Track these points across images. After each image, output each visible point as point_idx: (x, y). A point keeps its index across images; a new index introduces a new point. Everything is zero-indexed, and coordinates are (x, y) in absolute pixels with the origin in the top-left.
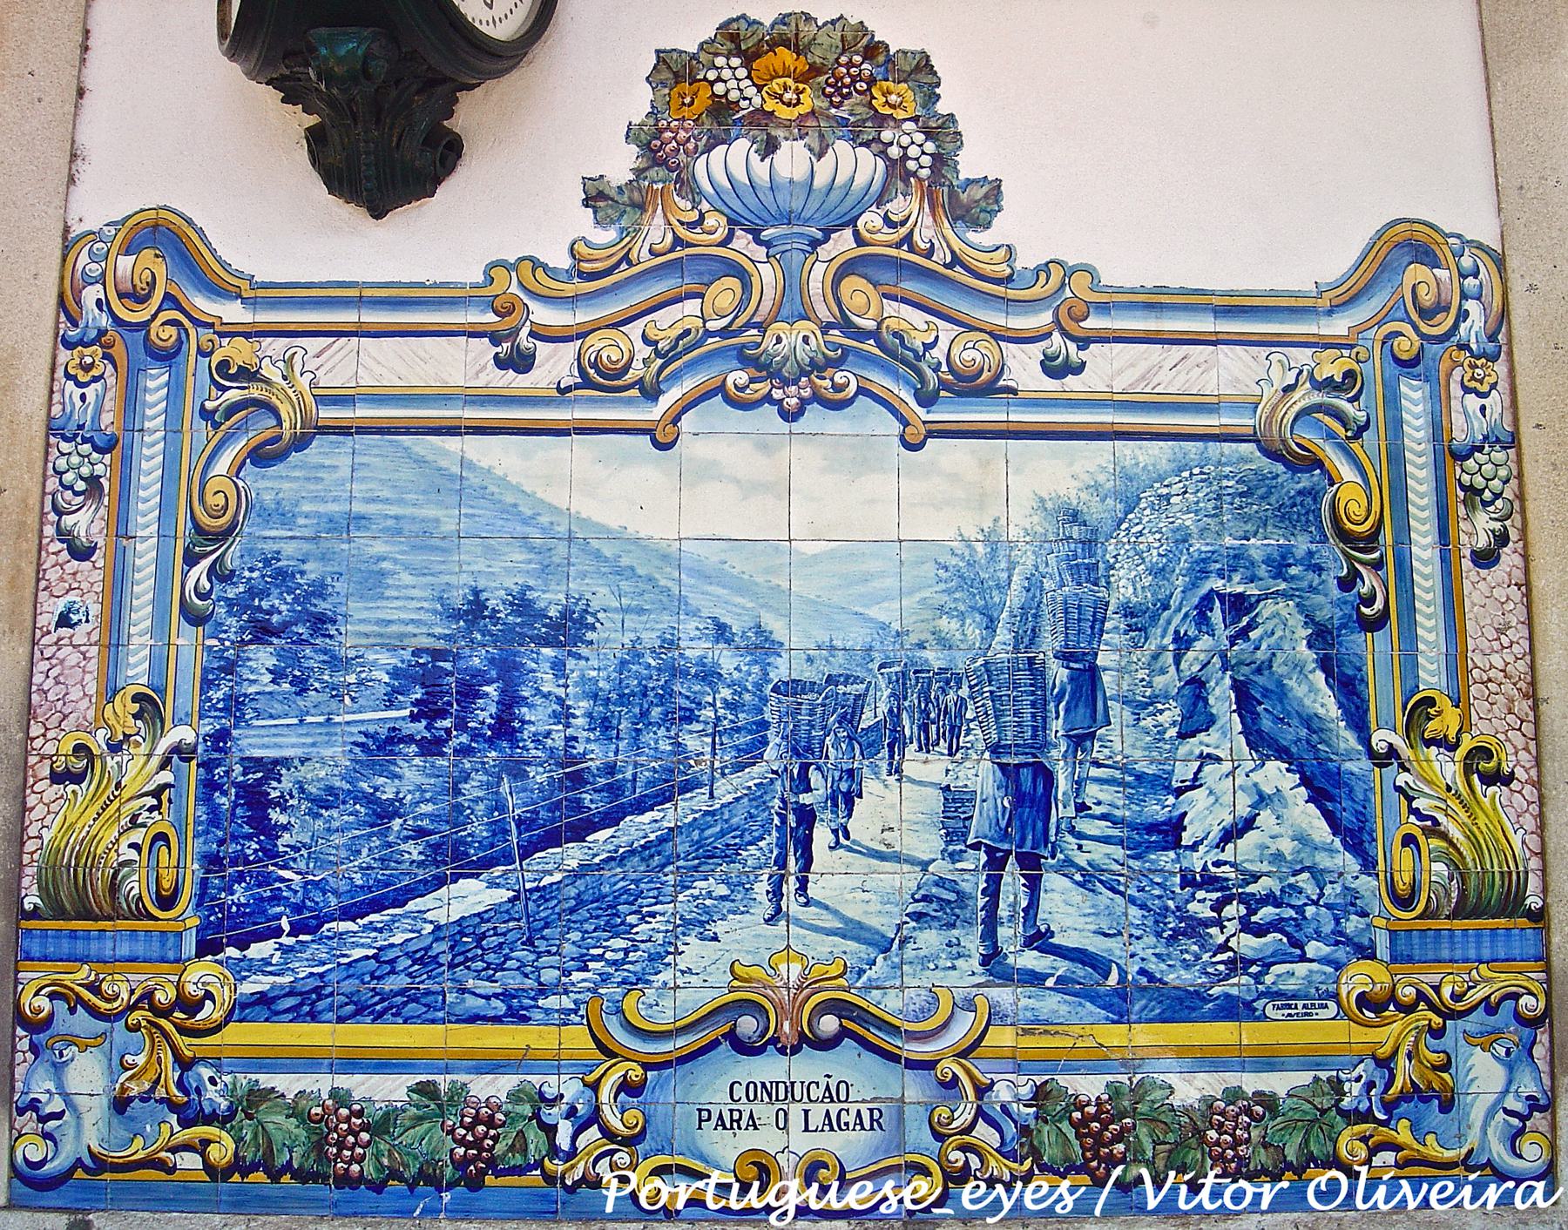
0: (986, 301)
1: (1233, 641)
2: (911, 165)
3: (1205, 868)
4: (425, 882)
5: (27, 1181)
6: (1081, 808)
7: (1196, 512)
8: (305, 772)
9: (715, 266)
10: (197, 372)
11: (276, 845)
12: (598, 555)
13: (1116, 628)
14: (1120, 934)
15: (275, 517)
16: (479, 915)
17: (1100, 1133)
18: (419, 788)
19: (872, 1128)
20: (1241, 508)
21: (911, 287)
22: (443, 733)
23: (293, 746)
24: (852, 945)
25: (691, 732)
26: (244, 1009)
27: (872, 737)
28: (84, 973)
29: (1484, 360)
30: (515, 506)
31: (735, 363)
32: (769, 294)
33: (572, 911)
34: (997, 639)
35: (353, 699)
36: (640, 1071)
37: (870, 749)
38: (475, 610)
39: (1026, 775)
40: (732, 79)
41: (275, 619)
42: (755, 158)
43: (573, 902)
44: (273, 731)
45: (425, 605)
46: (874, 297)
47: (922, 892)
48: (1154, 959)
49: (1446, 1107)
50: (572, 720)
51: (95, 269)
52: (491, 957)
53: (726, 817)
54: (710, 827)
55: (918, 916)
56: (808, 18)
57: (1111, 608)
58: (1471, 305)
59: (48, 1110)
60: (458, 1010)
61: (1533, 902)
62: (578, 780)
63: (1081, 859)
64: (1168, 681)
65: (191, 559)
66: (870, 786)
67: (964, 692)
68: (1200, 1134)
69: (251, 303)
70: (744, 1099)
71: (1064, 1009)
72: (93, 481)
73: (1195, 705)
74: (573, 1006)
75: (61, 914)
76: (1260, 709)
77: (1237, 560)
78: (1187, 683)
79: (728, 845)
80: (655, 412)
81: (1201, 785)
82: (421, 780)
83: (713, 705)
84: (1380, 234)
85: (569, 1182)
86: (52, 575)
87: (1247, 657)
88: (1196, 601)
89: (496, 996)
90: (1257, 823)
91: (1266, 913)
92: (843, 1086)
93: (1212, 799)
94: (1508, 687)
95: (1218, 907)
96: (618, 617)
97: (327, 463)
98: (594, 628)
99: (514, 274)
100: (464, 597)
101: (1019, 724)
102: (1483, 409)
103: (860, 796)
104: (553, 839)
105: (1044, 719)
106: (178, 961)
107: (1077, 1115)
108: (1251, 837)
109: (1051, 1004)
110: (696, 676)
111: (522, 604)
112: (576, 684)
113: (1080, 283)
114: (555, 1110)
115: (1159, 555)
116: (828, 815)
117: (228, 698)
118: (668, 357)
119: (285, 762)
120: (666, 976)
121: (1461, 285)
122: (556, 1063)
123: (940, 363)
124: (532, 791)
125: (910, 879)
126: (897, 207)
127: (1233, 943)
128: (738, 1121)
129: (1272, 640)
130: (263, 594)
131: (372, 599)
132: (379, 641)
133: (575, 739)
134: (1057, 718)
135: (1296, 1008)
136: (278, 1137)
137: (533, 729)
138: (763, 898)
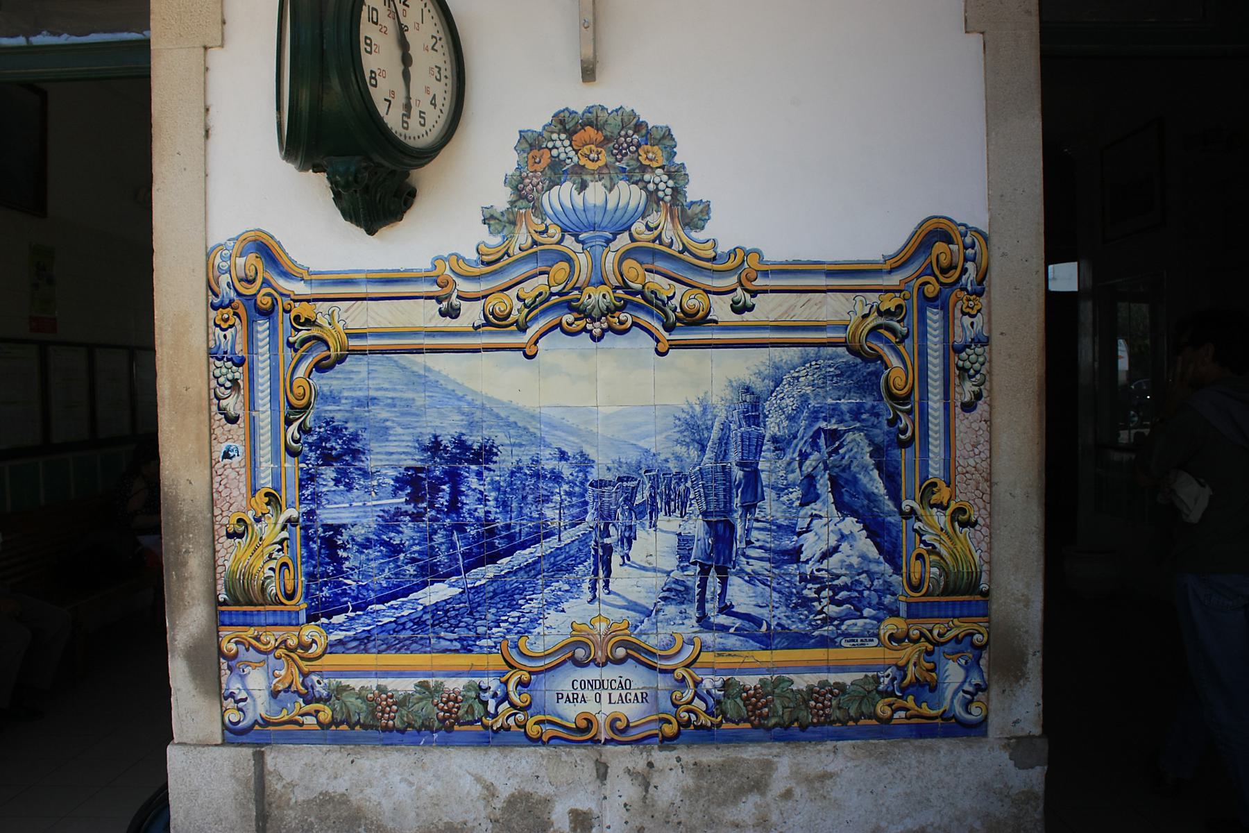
0: (701, 272)
1: (830, 455)
2: (661, 194)
3: (812, 572)
4: (417, 584)
5: (231, 731)
6: (749, 543)
7: (813, 386)
8: (354, 531)
9: (554, 256)
10: (283, 321)
12: (498, 416)
13: (769, 449)
14: (767, 606)
15: (330, 399)
16: (445, 601)
18: (412, 538)
19: (642, 702)
20: (837, 383)
21: (660, 265)
22: (422, 510)
23: (347, 518)
24: (632, 614)
25: (548, 508)
26: (331, 648)
27: (641, 508)
28: (252, 631)
29: (974, 296)
30: (454, 391)
31: (567, 310)
32: (584, 270)
33: (491, 598)
34: (706, 456)
35: (376, 493)
36: (528, 675)
37: (640, 515)
38: (435, 447)
39: (720, 526)
40: (562, 147)
41: (334, 453)
42: (575, 193)
43: (491, 594)
44: (337, 510)
45: (410, 444)
46: (641, 271)
47: (667, 587)
48: (785, 618)
49: (933, 689)
50: (487, 503)
51: (225, 265)
52: (452, 621)
53: (567, 550)
54: (559, 555)
55: (665, 599)
56: (603, 108)
57: (766, 439)
58: (970, 265)
59: (239, 697)
60: (437, 647)
61: (984, 587)
62: (492, 533)
63: (748, 569)
64: (796, 476)
65: (289, 423)
66: (640, 533)
67: (689, 484)
68: (806, 702)
69: (309, 282)
70: (579, 688)
71: (738, 643)
72: (234, 381)
73: (809, 489)
74: (493, 644)
75: (237, 603)
76: (843, 490)
77: (835, 411)
78: (805, 477)
79: (568, 565)
80: (524, 339)
81: (811, 531)
82: (413, 534)
83: (559, 493)
84: (921, 225)
85: (495, 728)
86: (218, 432)
87: (837, 463)
88: (811, 433)
89: (456, 640)
90: (840, 549)
91: (843, 594)
92: (628, 682)
93: (817, 537)
94: (977, 476)
95: (818, 592)
96: (509, 448)
97: (355, 370)
98: (497, 455)
99: (447, 263)
100: (430, 439)
101: (717, 501)
102: (972, 324)
103: (635, 539)
105: (731, 497)
106: (298, 625)
107: (745, 695)
108: (837, 557)
109: (732, 641)
110: (550, 478)
111: (460, 443)
112: (489, 484)
113: (752, 261)
114: (487, 694)
115: (793, 409)
116: (619, 549)
117: (313, 494)
118: (531, 307)
119: (344, 526)
120: (539, 629)
121: (965, 254)
123: (676, 308)
124: (469, 539)
125: (659, 581)
126: (653, 219)
127: (825, 610)
128: (576, 699)
129: (851, 454)
130: (327, 440)
131: (383, 441)
132: (387, 463)
133: (490, 512)
134: (737, 496)
136: (352, 708)
137: (468, 507)
138: (587, 591)
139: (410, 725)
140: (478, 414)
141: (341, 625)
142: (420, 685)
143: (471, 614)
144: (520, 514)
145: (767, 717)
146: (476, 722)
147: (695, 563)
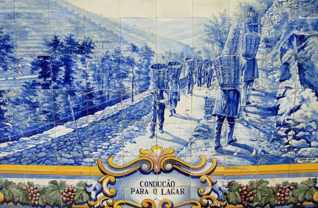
3: (284, 121)
4: (48, 126)
6: (248, 103)
7: (291, 8)
8: (9, 94)
11: (4, 116)
12: (94, 24)
13: (262, 46)
14: (257, 140)
16: (64, 136)
17: (247, 194)
18: (43, 99)
19: (181, 194)
20: (305, 6)
22: (49, 82)
23: (5, 87)
24: (176, 144)
25: (125, 81)
27: (183, 82)
30: (66, 8)
33: (92, 135)
34: (224, 50)
35: (21, 72)
36: (114, 178)
37: (182, 86)
38: (56, 43)
39: (231, 93)
43: (91, 132)
45: (40, 42)
47: (198, 129)
48: (266, 147)
50: (88, 78)
52: (69, 148)
53: (137, 107)
54: (132, 110)
55: (196, 136)
57: (261, 40)
60: (61, 162)
62: (91, 96)
63: (247, 119)
66: (182, 97)
67: (213, 67)
68: (274, 193)
70: (144, 186)
71: (238, 162)
73: (285, 71)
74: (93, 161)
76: (305, 72)
77: (303, 24)
78: (284, 64)
79: (138, 115)
81: (285, 96)
82: (44, 96)
83: (132, 72)
85: (95, 207)
87: (303, 56)
88: (288, 37)
89: (71, 158)
90: (301, 107)
91: (301, 134)
92: (173, 183)
93: (288, 100)
95: (287, 132)
96: (101, 44)
98: (93, 48)
100: (52, 38)
101: (230, 78)
103: (179, 100)
104: (84, 114)
105: (238, 76)
107: (240, 190)
108: (299, 112)
109: (235, 160)
110: (127, 63)
111: (70, 41)
112: (89, 66)
114: (90, 189)
115: (278, 22)
116: (169, 106)
120: (120, 153)
122: (90, 177)
124: (77, 99)
125: (194, 125)
127: (290, 142)
128: (143, 192)
129: (311, 50)
131: (24, 40)
132: (27, 53)
133: (89, 83)
134: (242, 75)
135: (306, 160)
136: (15, 194)
137: (76, 80)
138: (149, 131)
139: (47, 204)
140: (82, 22)
141: (5, 148)
142: (53, 182)
143: (80, 143)
144: (108, 85)
145: (252, 202)
146: (84, 203)
147: (215, 115)
